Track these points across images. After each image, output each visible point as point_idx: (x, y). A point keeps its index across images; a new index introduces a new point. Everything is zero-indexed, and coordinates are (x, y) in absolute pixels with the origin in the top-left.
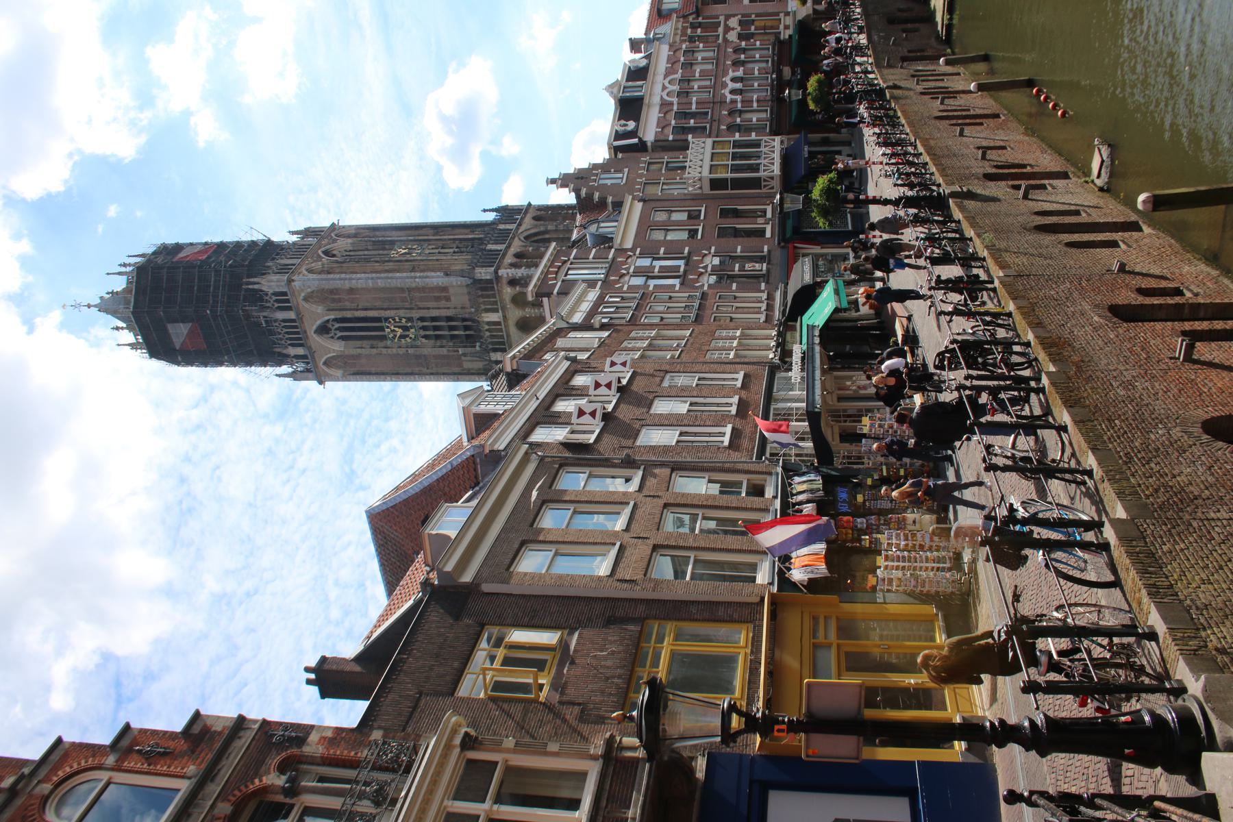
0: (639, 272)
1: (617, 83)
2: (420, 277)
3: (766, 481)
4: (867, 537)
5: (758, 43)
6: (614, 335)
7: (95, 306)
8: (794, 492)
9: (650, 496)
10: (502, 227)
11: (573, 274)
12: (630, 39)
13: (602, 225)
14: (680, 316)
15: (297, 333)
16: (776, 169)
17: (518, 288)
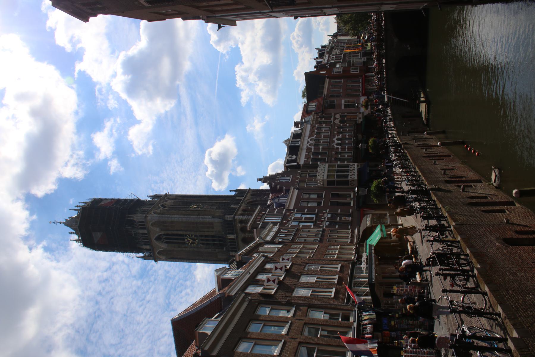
0: (296, 219)
1: (288, 140)
2: (201, 218)
3: (350, 314)
4: (396, 341)
5: (348, 125)
6: (284, 246)
8: (363, 319)
9: (298, 319)
10: (237, 198)
11: (267, 220)
12: (295, 122)
13: (281, 199)
14: (313, 239)
16: (355, 177)
17: (243, 225)
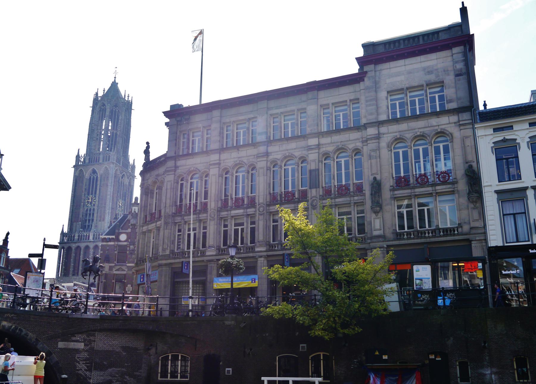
7: (115, 80)
15: (94, 162)
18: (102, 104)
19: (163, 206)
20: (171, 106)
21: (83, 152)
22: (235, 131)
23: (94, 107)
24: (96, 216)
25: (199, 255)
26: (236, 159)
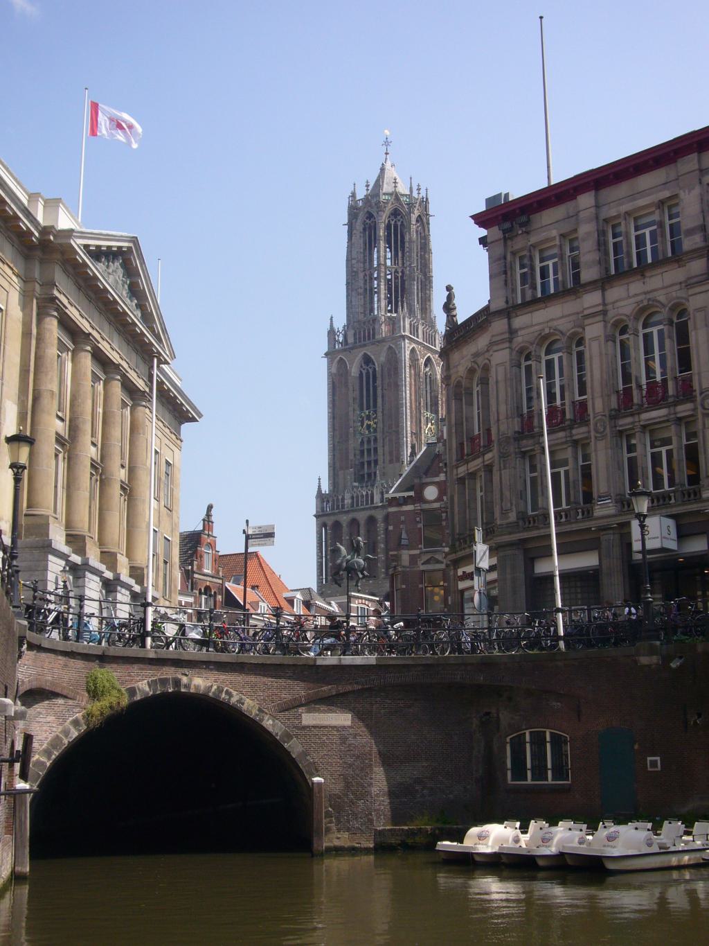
2: (407, 441)
18: (367, 215)
19: (493, 418)
20: (488, 201)
21: (340, 322)
22: (633, 234)
23: (351, 225)
24: (382, 454)
25: (580, 516)
26: (640, 298)
